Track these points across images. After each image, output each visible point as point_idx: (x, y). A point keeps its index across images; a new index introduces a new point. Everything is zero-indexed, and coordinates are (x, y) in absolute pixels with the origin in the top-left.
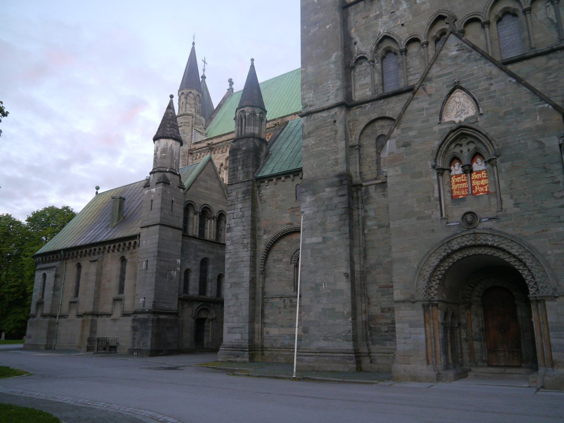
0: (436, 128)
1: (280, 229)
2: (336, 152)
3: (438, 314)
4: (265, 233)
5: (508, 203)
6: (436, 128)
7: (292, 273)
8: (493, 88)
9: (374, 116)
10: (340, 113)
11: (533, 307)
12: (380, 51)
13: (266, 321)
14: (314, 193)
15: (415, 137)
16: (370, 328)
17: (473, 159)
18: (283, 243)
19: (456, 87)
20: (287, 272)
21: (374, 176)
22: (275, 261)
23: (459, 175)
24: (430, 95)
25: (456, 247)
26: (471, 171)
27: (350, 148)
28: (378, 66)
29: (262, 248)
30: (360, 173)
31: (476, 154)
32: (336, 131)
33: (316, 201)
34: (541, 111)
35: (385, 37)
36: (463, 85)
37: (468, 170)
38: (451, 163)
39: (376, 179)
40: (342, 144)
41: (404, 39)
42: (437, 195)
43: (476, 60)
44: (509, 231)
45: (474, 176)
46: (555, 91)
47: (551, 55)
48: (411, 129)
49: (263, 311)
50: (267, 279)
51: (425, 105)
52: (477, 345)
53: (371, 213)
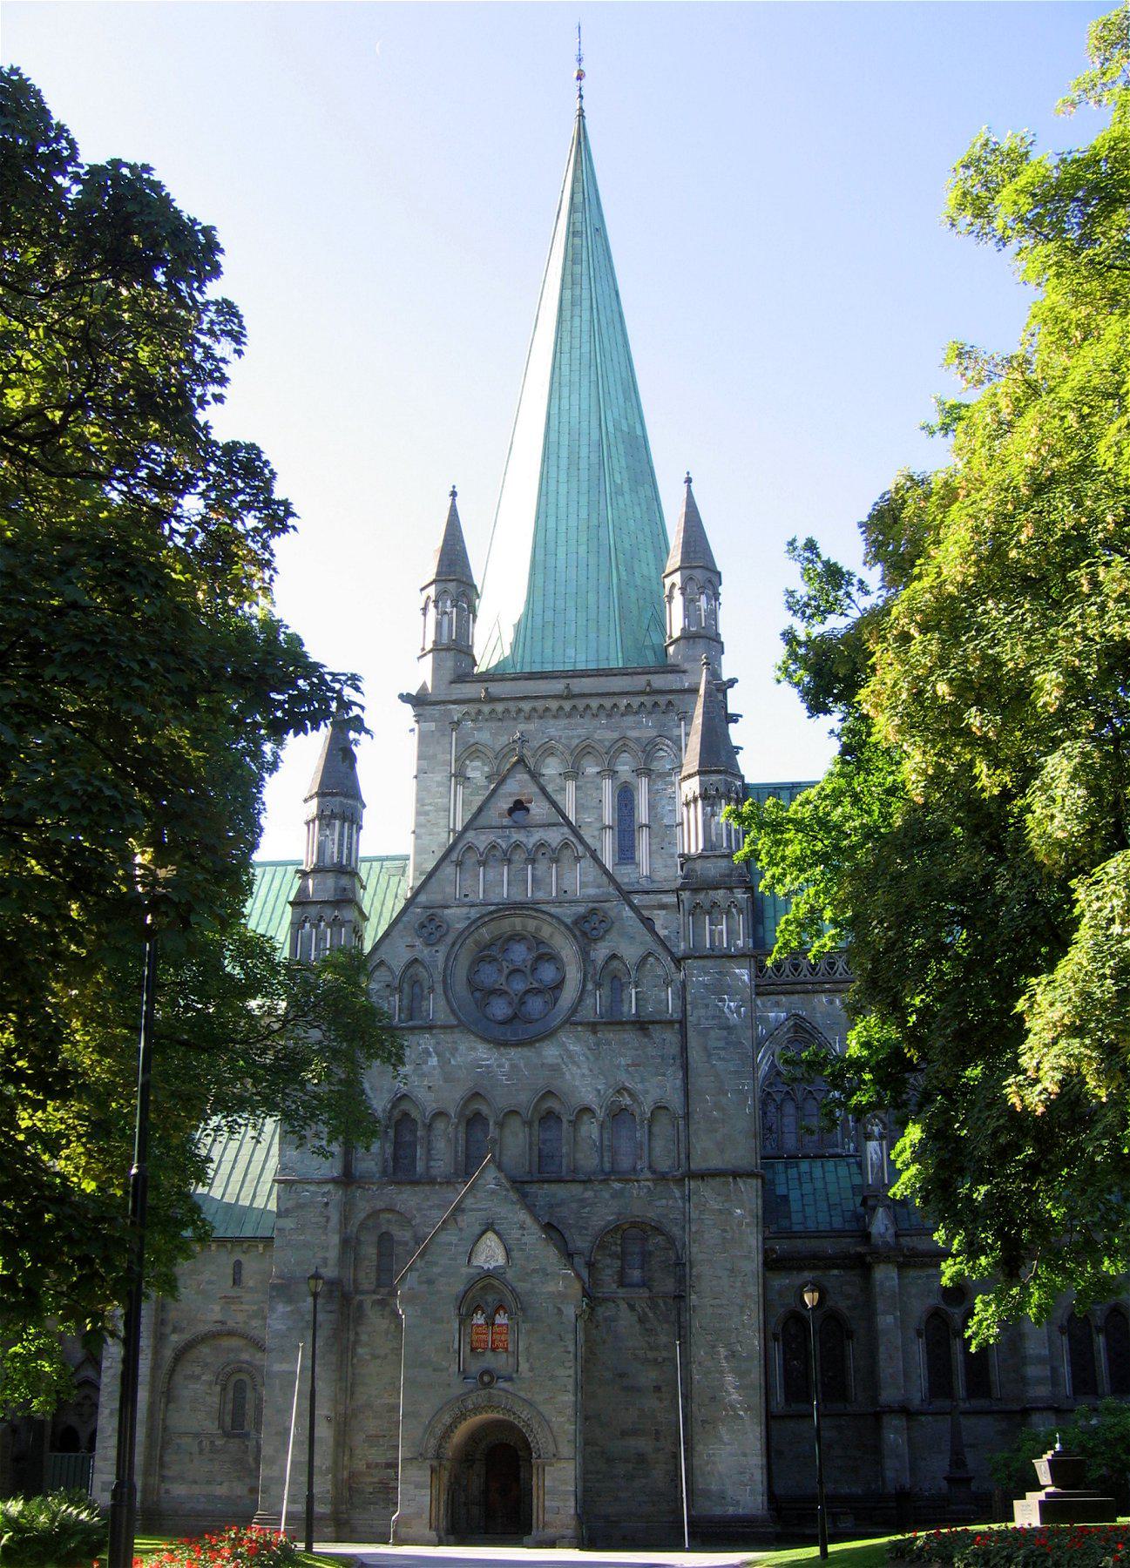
0: (464, 1270)
1: (203, 1328)
2: (325, 1248)
3: (445, 1475)
4: (174, 1331)
5: (524, 1366)
6: (464, 1270)
7: (217, 1400)
8: (525, 1239)
9: (380, 1205)
10: (337, 1194)
11: (534, 1471)
12: (396, 1113)
13: (167, 1473)
14: (290, 1300)
15: (440, 1275)
16: (350, 1488)
17: (497, 1311)
18: (205, 1350)
19: (489, 1227)
20: (208, 1398)
21: (372, 1287)
22: (186, 1377)
23: (481, 1325)
24: (461, 1230)
25: (471, 1406)
26: (493, 1324)
27: (345, 1242)
28: (391, 1132)
29: (168, 1353)
30: (355, 1280)
31: (500, 1307)
32: (328, 1219)
33: (292, 1311)
34: (566, 1276)
35: (405, 1096)
36: (497, 1228)
37: (490, 1322)
38: (475, 1311)
39: (374, 1292)
40: (335, 1239)
41: (429, 1109)
42: (456, 1346)
43: (513, 1203)
44: (522, 1394)
45: (496, 1329)
46: (586, 1229)
47: (588, 1185)
48: (435, 1264)
49: (161, 1456)
50: (172, 1406)
51: (454, 1239)
52: (475, 1510)
53: (364, 1338)
